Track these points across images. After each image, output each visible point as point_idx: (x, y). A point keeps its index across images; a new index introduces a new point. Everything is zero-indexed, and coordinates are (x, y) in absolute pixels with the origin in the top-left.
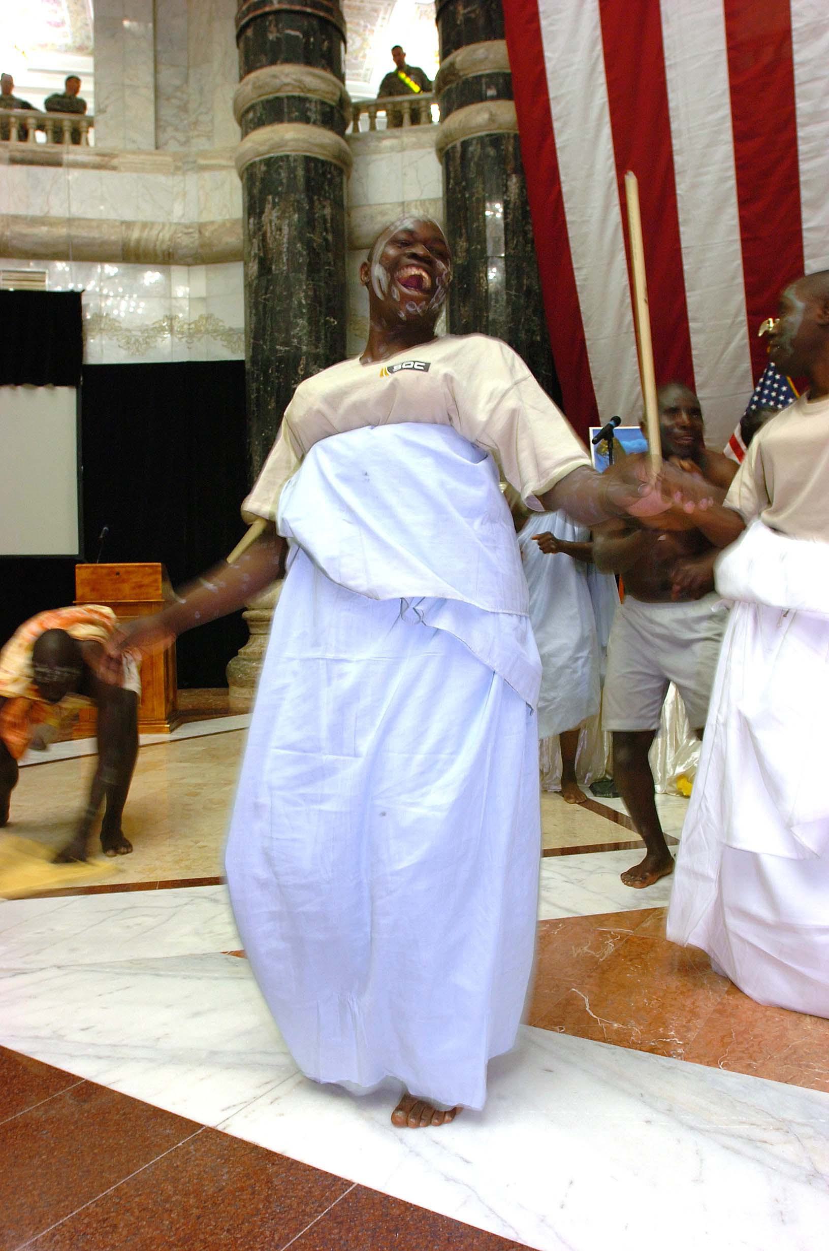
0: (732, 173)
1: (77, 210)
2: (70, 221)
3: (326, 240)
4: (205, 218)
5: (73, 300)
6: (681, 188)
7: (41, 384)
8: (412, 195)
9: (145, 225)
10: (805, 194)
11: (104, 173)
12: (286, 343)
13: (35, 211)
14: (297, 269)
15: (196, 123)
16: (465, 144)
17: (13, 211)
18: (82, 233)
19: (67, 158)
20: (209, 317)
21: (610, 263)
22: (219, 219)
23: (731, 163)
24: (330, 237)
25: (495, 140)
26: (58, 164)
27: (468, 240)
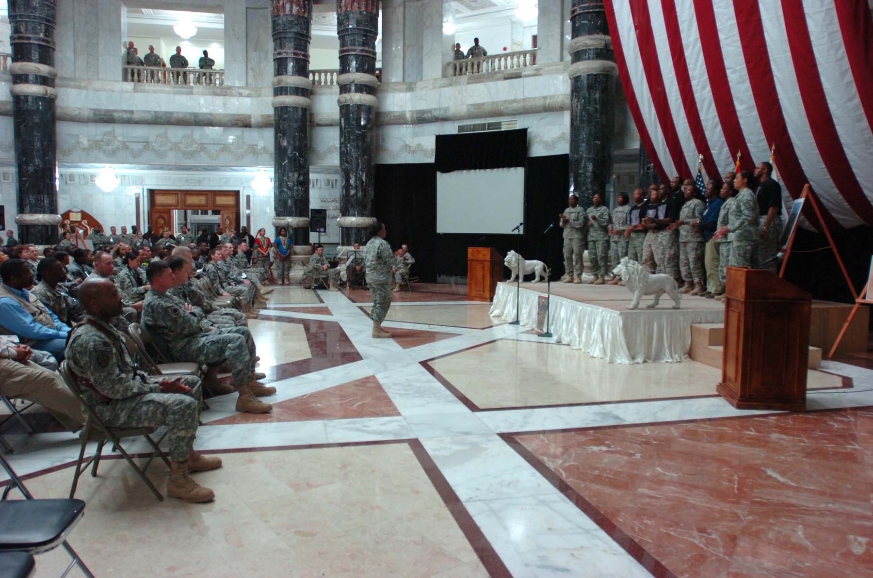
0: (679, 96)
1: (527, 95)
2: (524, 100)
3: (596, 108)
5: (524, 132)
7: (511, 166)
9: (552, 97)
11: (536, 77)
12: (578, 154)
13: (511, 98)
14: (582, 122)
17: (504, 99)
18: (528, 104)
19: (524, 73)
21: (656, 127)
23: (678, 93)
24: (598, 107)
26: (520, 77)
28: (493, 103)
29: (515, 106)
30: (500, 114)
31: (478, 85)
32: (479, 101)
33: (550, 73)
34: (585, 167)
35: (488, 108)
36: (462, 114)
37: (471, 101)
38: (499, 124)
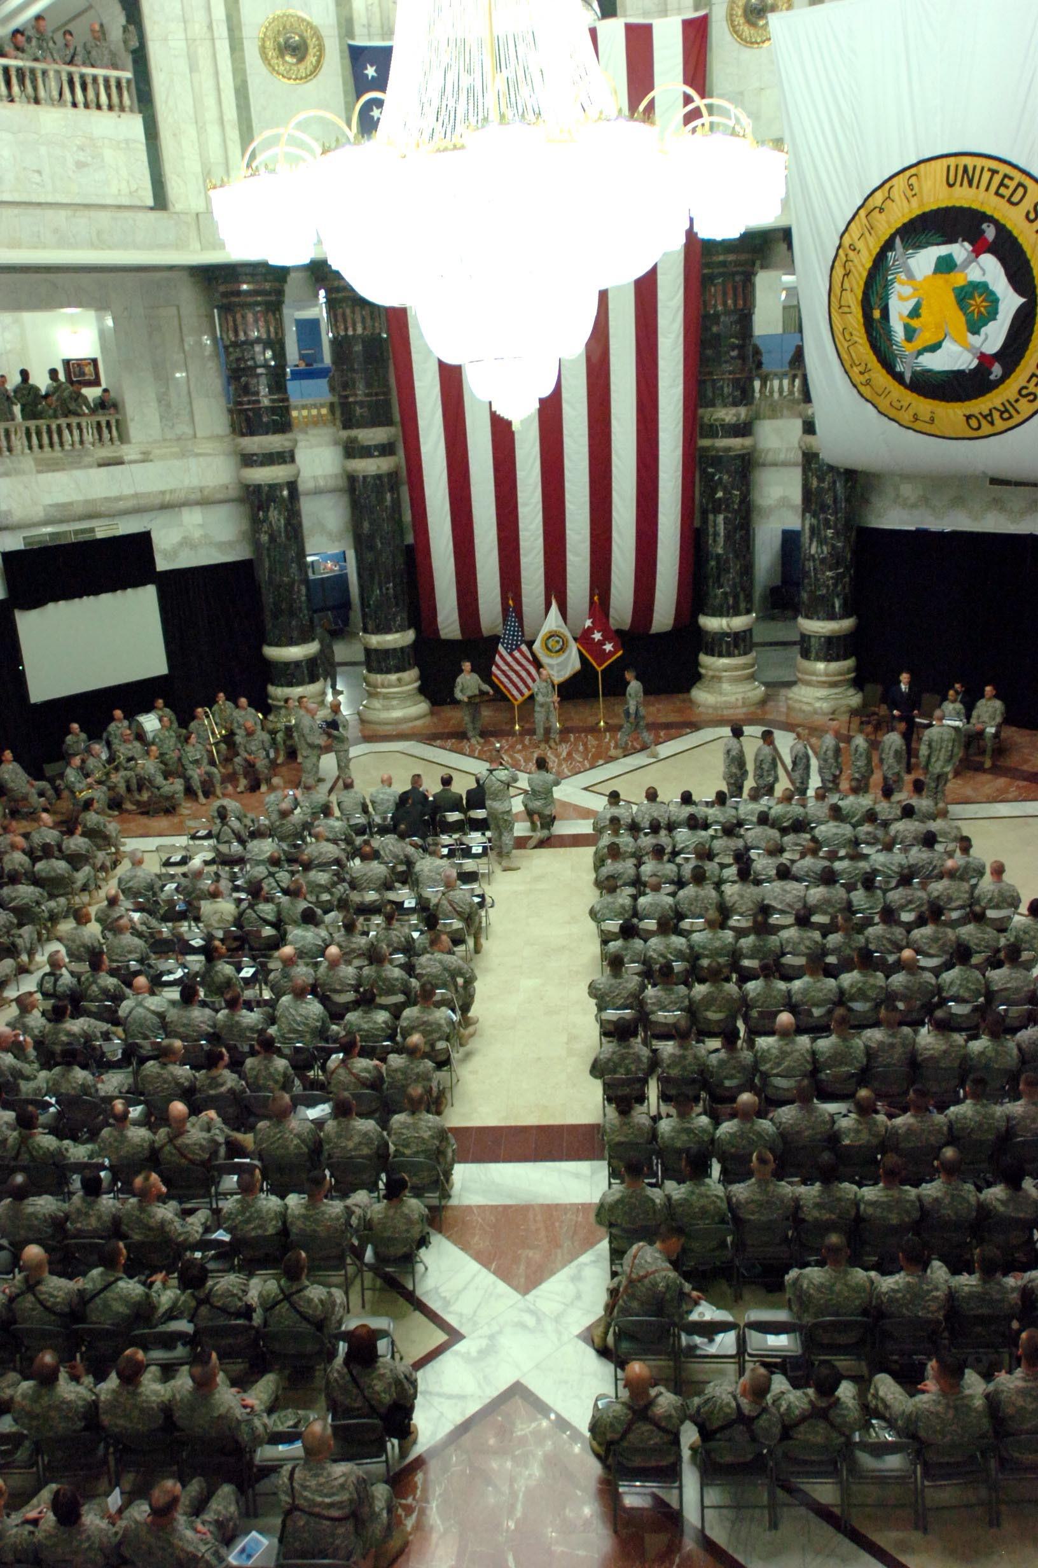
2: (136, 495)
4: (203, 484)
6: (477, 541)
8: (319, 472)
9: (171, 492)
10: (522, 552)
13: (113, 493)
14: (288, 538)
15: (178, 415)
16: (365, 477)
18: (142, 502)
19: (126, 458)
20: (206, 536)
22: (211, 484)
25: (379, 477)
26: (119, 462)
27: (371, 524)
28: (87, 501)
29: (121, 505)
30: (90, 517)
31: (58, 475)
32: (62, 499)
33: (163, 457)
34: (299, 591)
35: (79, 510)
36: (36, 519)
37: (48, 500)
38: (92, 530)
